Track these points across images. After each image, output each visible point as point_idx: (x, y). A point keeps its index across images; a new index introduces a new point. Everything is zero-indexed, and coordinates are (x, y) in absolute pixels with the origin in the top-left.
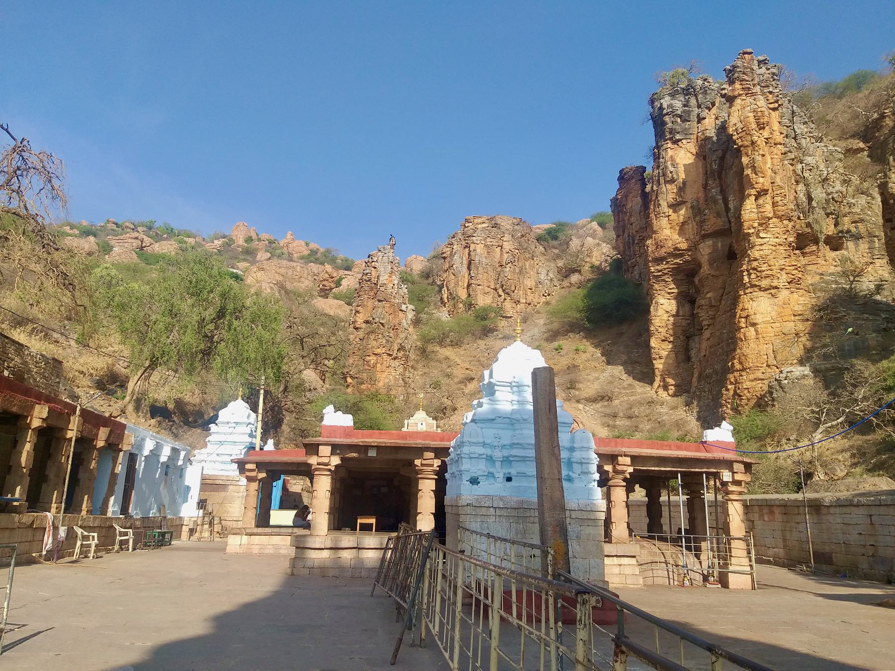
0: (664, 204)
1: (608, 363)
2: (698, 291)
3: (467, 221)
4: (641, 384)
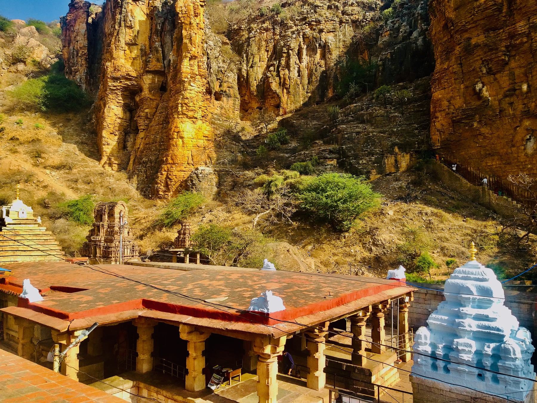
1: (64, 141)
4: (92, 160)
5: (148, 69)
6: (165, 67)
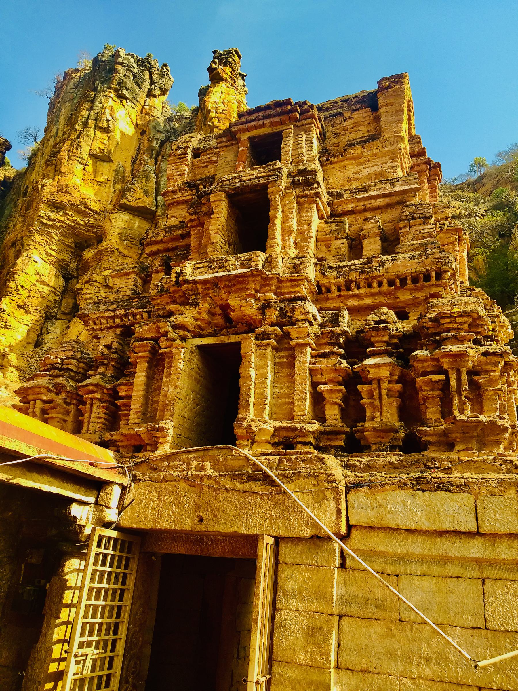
2: (84, 267)
6: (157, 206)
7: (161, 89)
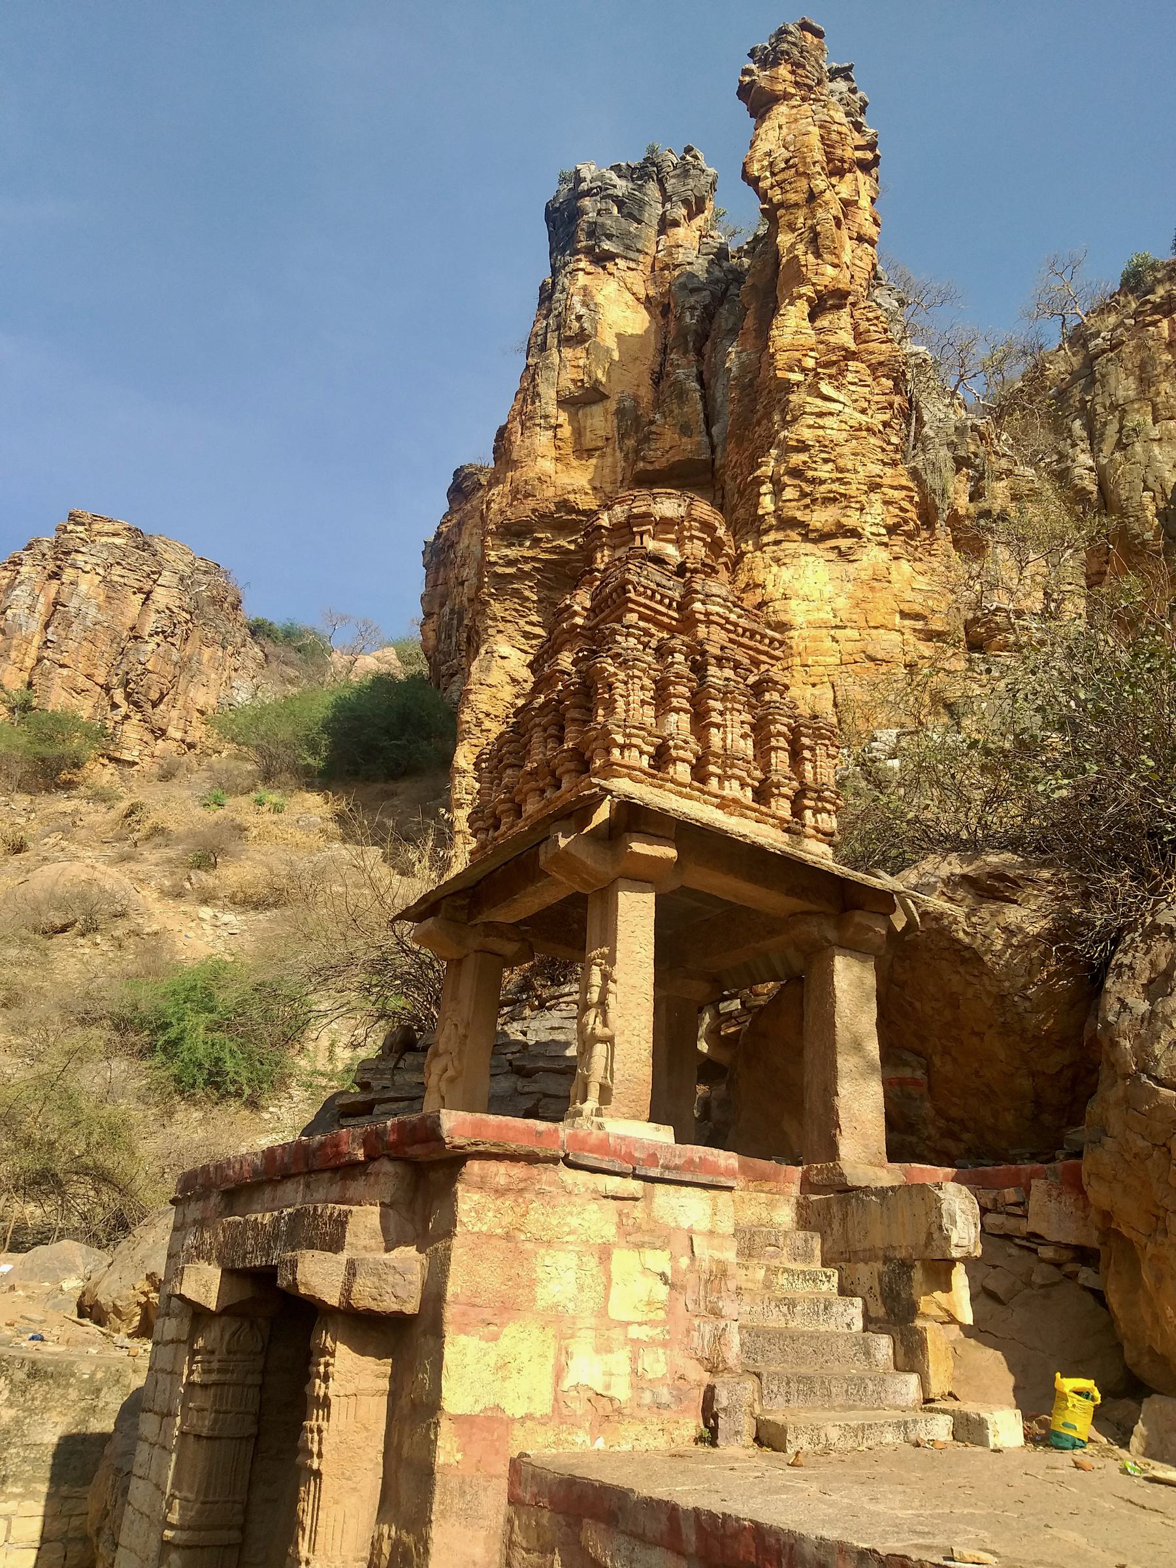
0: (548, 394)
3: (73, 518)
5: (641, 464)
7: (686, 202)
